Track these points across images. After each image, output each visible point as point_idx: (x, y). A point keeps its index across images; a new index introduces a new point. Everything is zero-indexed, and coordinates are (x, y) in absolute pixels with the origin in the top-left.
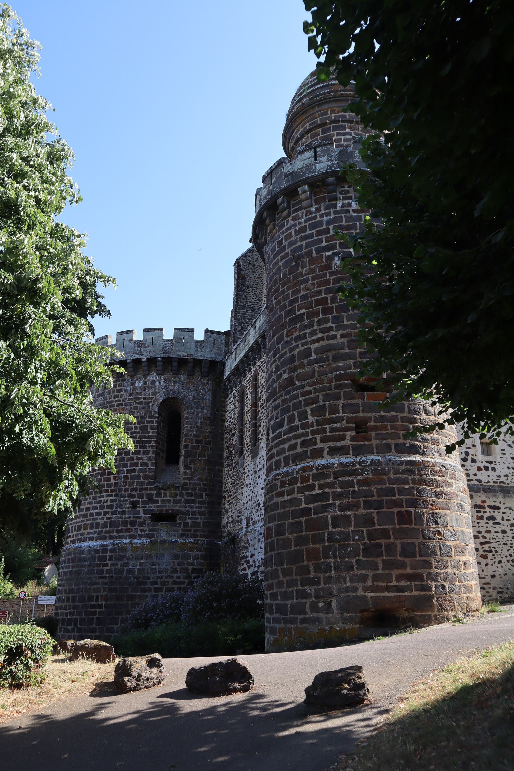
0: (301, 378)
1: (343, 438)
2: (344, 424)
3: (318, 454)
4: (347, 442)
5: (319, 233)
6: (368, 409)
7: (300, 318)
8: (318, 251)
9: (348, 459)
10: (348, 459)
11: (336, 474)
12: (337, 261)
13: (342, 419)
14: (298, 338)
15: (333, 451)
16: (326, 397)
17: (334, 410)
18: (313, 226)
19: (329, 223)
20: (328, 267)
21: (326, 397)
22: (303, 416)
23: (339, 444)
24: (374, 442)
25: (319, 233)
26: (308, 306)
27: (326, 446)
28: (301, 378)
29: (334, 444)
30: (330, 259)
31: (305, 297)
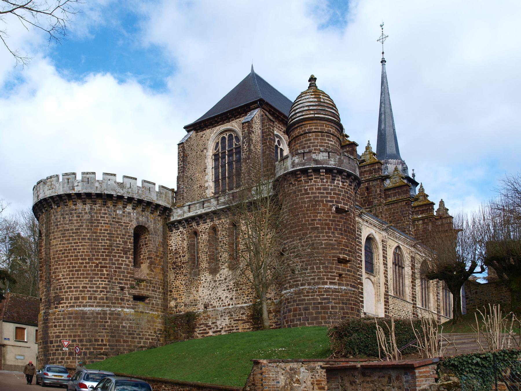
1: (334, 279)
2: (335, 274)
3: (326, 283)
4: (336, 281)
6: (343, 270)
9: (337, 287)
10: (337, 287)
11: (333, 292)
13: (334, 272)
15: (331, 283)
16: (329, 263)
22: (318, 268)
23: (333, 281)
24: (344, 282)
27: (328, 281)
29: (331, 281)
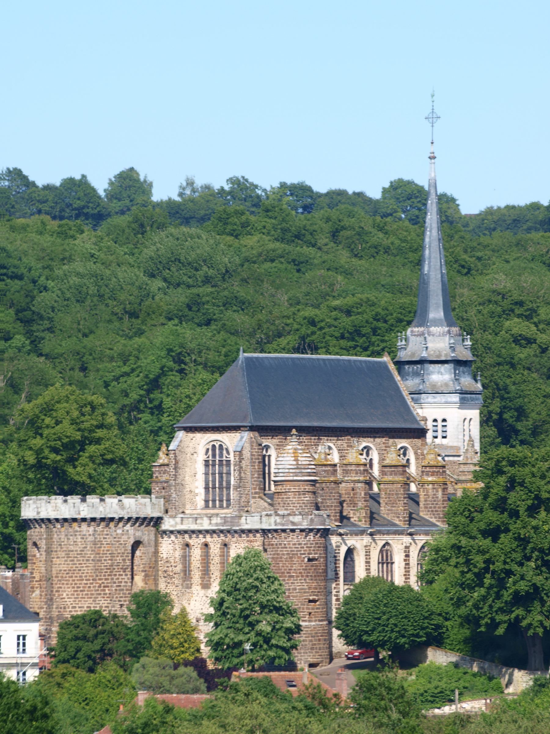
0: (293, 596)
5: (301, 548)
6: (313, 609)
7: (293, 576)
8: (301, 554)
12: (306, 560)
14: (292, 583)
16: (302, 605)
17: (303, 609)
18: (299, 544)
19: (305, 544)
20: (303, 561)
21: (302, 605)
25: (301, 548)
26: (296, 573)
28: (293, 596)
30: (304, 558)
31: (295, 570)
